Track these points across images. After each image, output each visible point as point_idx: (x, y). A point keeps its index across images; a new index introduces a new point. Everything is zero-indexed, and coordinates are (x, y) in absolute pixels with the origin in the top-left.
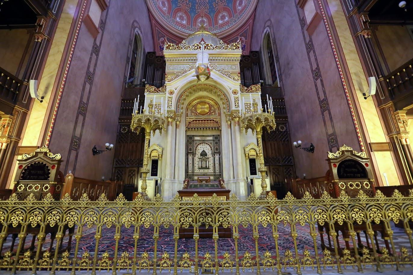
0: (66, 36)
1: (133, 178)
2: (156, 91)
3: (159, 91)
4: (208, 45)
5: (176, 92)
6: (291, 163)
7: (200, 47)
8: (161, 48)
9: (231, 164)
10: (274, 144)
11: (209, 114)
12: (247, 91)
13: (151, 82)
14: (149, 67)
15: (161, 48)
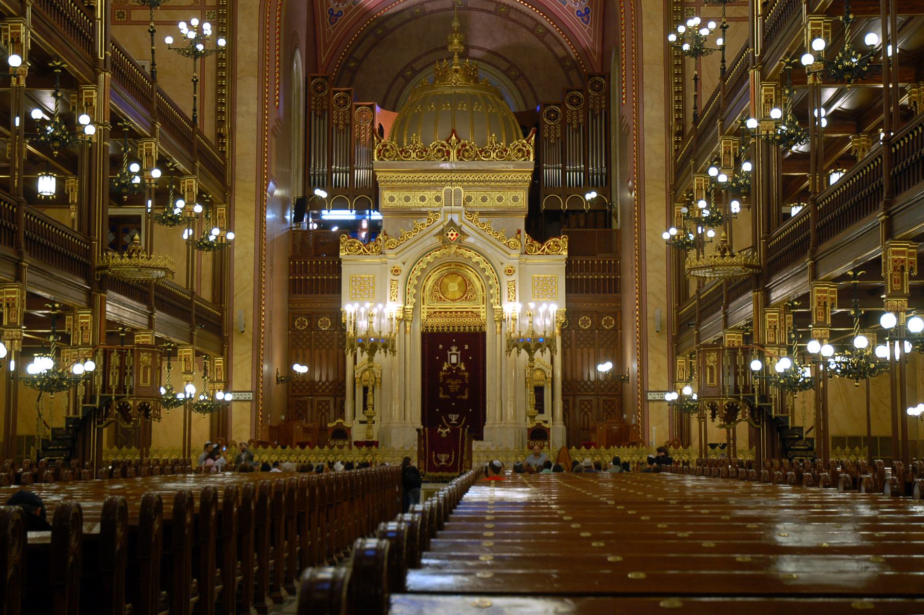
0: (252, 226)
1: (325, 416)
2: (362, 250)
3: (369, 250)
4: (464, 146)
5: (405, 269)
6: (616, 390)
7: (448, 153)
8: (332, 14)
9: (498, 397)
10: (589, 355)
11: (464, 298)
12: (539, 252)
13: (325, 170)
14: (315, 120)
15: (332, 14)
